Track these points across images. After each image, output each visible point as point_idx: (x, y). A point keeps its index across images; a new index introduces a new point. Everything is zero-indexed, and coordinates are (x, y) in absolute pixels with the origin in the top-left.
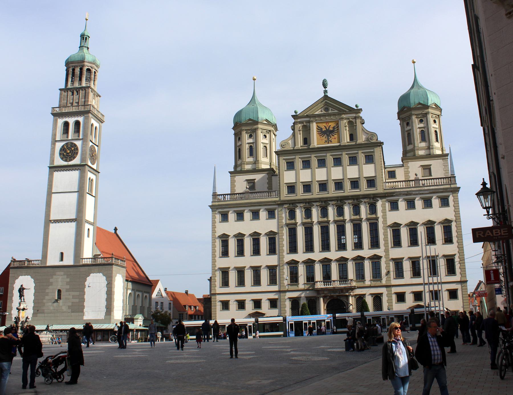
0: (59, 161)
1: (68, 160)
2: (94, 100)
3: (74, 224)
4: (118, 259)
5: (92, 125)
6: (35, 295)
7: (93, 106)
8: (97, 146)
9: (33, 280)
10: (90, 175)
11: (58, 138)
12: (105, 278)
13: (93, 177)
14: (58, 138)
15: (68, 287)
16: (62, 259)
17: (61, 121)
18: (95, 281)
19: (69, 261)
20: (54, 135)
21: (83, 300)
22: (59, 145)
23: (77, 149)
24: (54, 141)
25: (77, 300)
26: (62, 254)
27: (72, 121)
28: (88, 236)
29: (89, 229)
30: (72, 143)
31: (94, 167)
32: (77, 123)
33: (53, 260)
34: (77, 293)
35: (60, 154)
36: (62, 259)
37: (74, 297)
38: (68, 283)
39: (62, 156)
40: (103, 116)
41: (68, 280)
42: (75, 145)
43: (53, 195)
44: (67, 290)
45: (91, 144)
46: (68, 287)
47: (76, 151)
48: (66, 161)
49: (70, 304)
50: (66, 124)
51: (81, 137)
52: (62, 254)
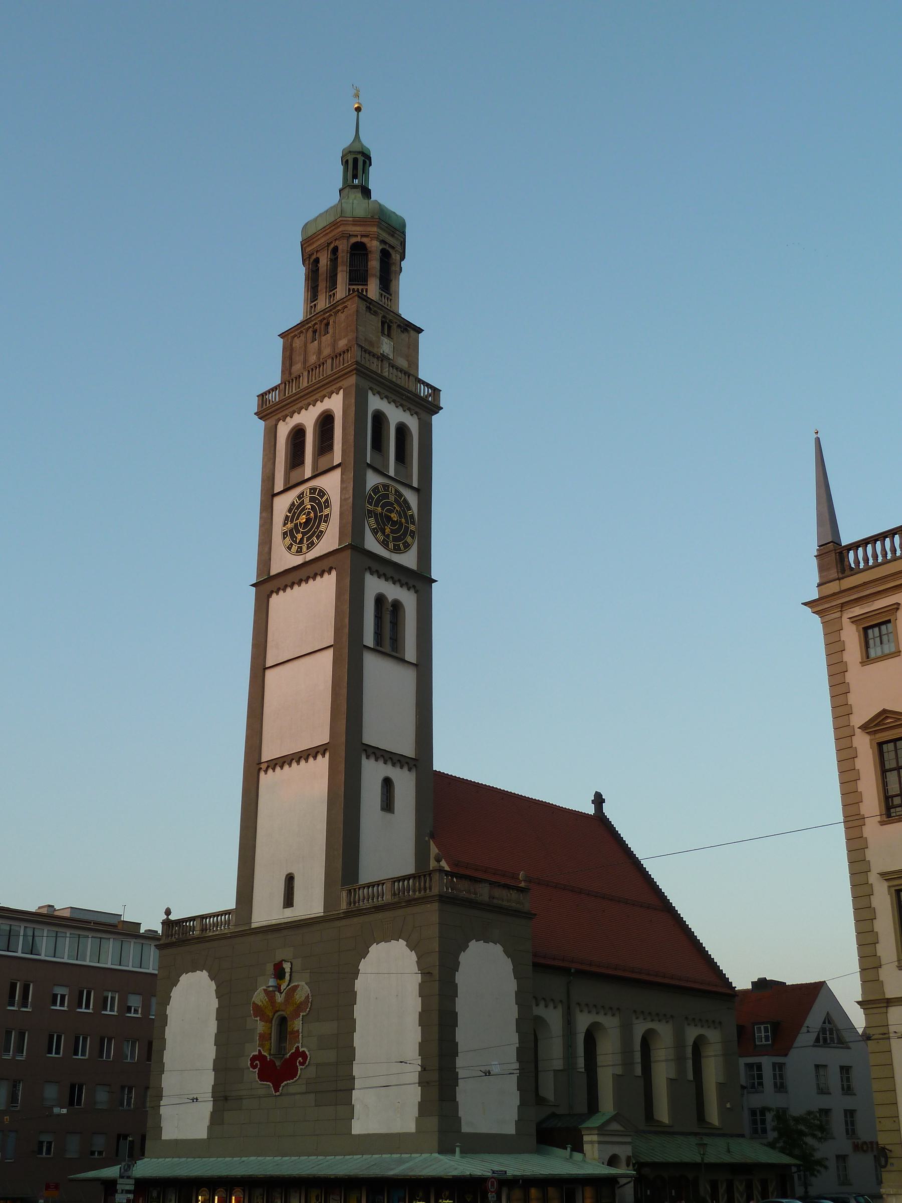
0: (284, 559)
1: (304, 549)
2: (385, 340)
4: (481, 881)
5: (379, 419)
6: (219, 1042)
7: (383, 358)
8: (417, 490)
9: (213, 986)
10: (374, 586)
11: (279, 486)
12: (413, 956)
13: (393, 592)
14: (277, 489)
16: (289, 902)
17: (284, 430)
19: (311, 902)
20: (268, 479)
21: (347, 1054)
22: (281, 505)
23: (327, 504)
24: (269, 496)
26: (290, 879)
27: (308, 418)
28: (388, 805)
29: (387, 783)
30: (313, 490)
31: (409, 559)
32: (326, 420)
33: (267, 910)
35: (285, 534)
36: (289, 902)
39: (288, 540)
40: (436, 391)
42: (322, 493)
43: (268, 673)
45: (372, 480)
47: (326, 512)
48: (299, 551)
50: (298, 434)
51: (337, 458)
52: (290, 879)
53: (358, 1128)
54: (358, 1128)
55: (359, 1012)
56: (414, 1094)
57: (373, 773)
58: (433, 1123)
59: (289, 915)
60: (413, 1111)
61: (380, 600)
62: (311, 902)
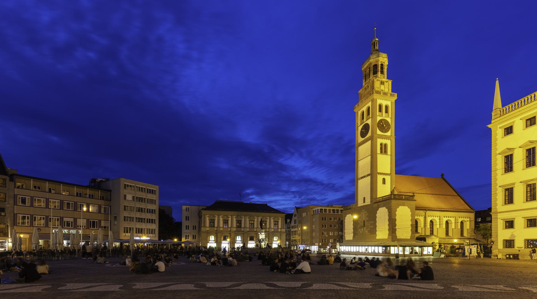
3: (369, 177)
15: (367, 219)
16: (364, 202)
18: (382, 213)
25: (372, 227)
26: (364, 198)
34: (372, 222)
36: (364, 202)
37: (371, 225)
38: (367, 216)
41: (367, 214)
44: (368, 221)
46: (367, 219)
49: (369, 229)
52: (364, 198)
53: (377, 238)
54: (377, 238)
55: (377, 220)
56: (387, 232)
57: (380, 178)
58: (391, 237)
59: (364, 204)
60: (387, 235)
61: (381, 144)
62: (368, 202)
